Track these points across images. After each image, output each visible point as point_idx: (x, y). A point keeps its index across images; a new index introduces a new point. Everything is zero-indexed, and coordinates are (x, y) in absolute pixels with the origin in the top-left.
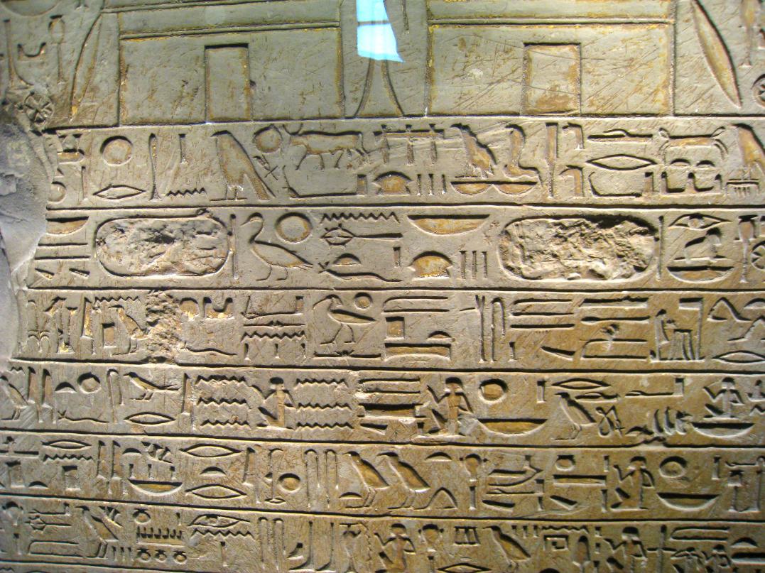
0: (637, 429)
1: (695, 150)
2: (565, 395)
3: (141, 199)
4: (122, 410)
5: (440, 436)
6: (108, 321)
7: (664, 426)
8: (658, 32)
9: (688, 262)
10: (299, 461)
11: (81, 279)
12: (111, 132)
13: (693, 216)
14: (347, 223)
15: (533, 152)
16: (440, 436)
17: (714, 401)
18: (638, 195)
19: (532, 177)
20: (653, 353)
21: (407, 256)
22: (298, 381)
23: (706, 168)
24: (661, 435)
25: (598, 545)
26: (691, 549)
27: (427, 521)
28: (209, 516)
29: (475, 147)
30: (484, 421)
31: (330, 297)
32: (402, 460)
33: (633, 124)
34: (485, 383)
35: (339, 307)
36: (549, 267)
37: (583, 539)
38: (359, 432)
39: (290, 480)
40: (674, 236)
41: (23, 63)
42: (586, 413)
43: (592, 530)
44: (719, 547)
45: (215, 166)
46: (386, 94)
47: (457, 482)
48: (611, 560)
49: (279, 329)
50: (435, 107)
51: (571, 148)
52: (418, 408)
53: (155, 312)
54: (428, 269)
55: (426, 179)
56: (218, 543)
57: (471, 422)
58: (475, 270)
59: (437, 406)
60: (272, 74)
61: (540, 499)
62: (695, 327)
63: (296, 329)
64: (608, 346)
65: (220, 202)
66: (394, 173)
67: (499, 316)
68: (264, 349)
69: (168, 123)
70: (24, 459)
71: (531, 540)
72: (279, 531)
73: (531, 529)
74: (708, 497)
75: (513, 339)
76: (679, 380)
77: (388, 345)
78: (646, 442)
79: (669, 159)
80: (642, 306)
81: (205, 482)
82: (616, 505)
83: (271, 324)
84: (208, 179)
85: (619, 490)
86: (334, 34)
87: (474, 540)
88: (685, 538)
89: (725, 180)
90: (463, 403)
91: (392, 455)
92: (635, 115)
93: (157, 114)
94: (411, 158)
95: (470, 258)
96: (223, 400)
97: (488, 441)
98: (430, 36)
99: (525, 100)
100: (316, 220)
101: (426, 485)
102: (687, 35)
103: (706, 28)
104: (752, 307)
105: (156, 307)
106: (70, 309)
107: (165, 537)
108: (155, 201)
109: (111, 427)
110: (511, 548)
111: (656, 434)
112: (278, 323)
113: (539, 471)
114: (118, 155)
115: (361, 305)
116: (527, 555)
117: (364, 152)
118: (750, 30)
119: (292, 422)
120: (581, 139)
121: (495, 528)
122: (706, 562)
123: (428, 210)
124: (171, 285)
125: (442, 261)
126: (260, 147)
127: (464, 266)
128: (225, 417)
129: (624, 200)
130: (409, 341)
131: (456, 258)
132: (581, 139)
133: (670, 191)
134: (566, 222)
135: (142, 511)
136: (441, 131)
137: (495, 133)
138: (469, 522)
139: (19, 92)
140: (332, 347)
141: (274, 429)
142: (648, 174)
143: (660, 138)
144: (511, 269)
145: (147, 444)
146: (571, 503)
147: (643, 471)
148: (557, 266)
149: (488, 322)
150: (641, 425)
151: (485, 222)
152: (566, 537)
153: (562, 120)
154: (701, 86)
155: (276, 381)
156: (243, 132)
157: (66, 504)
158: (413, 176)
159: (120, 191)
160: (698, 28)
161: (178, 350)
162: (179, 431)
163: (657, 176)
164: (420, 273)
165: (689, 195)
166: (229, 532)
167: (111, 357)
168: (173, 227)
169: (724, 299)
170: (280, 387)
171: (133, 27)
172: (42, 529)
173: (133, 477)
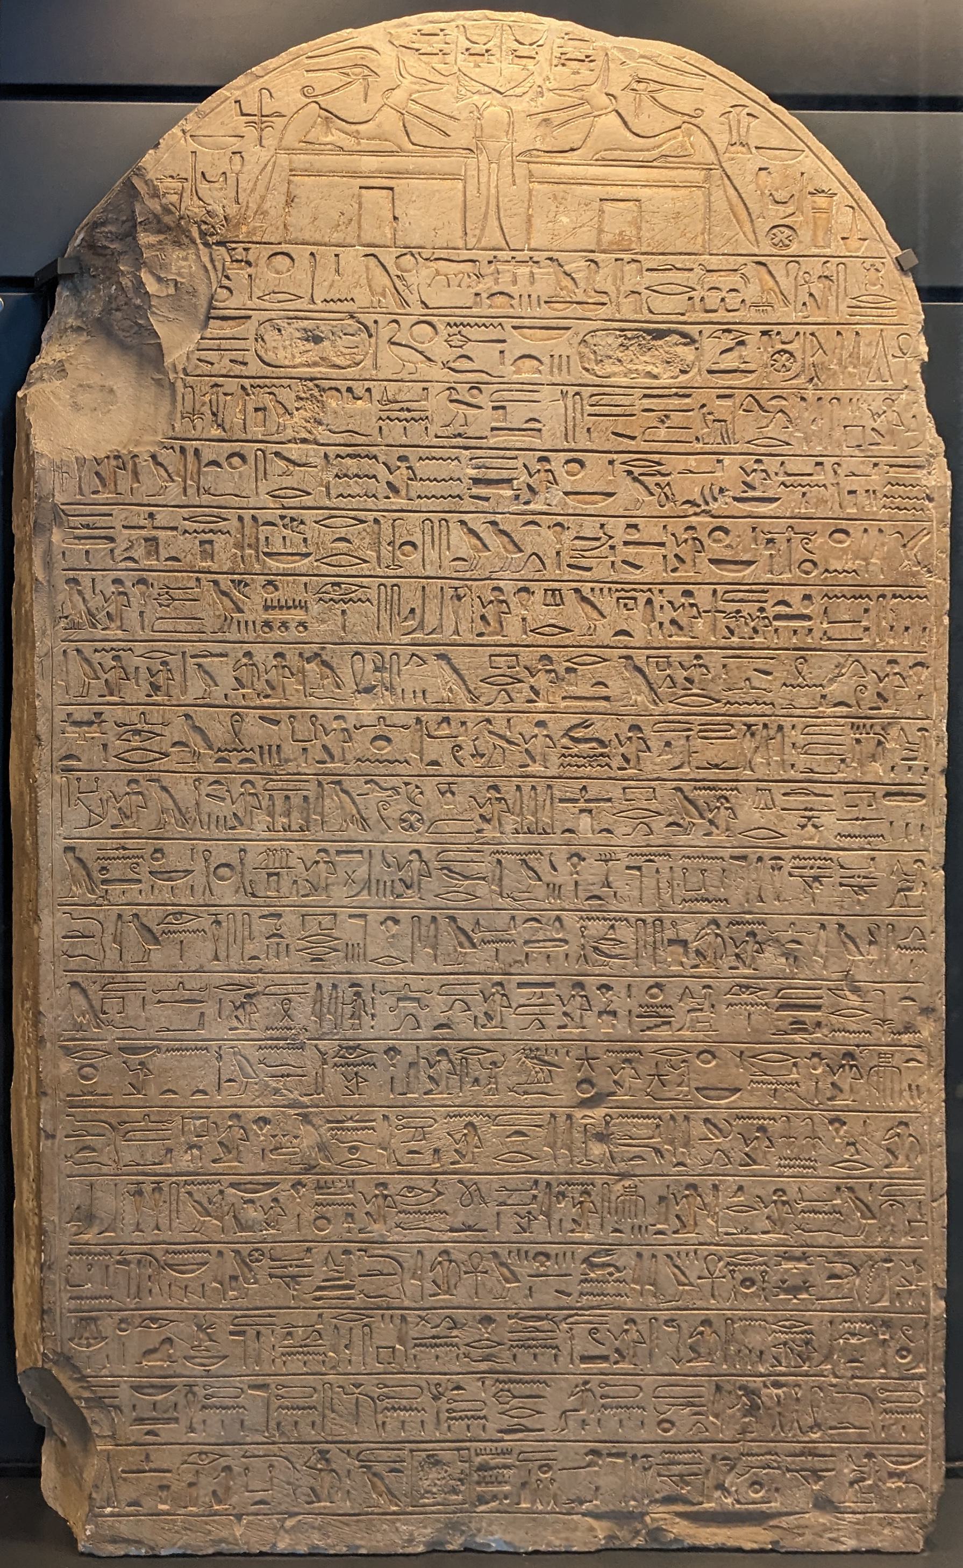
0: (687, 502)
1: (726, 281)
2: (630, 473)
3: (298, 304)
4: (264, 487)
5: (532, 507)
6: (261, 406)
7: (710, 500)
8: (699, 193)
9: (722, 367)
10: (418, 529)
11: (238, 369)
12: (278, 248)
13: (724, 331)
14: (465, 331)
15: (603, 279)
16: (532, 507)
17: (748, 479)
18: (683, 314)
19: (605, 299)
20: (697, 439)
21: (509, 359)
22: (421, 458)
23: (734, 294)
24: (707, 508)
25: (662, 607)
26: (738, 612)
27: (521, 584)
28: (333, 584)
29: (562, 276)
30: (566, 494)
31: (449, 389)
32: (501, 527)
33: (679, 261)
34: (568, 462)
35: (455, 397)
36: (616, 369)
37: (649, 602)
38: (468, 504)
39: (408, 548)
40: (711, 347)
41: (203, 186)
42: (647, 488)
43: (656, 592)
44: (762, 610)
45: (364, 281)
46: (498, 233)
47: (546, 547)
48: (673, 622)
49: (407, 415)
50: (533, 245)
51: (633, 278)
52: (515, 482)
53: (302, 399)
54: (524, 369)
55: (525, 299)
56: (339, 612)
57: (556, 495)
58: (560, 370)
59: (531, 481)
60: (411, 212)
61: (613, 563)
62: (729, 418)
63: (423, 414)
64: (662, 433)
65: (365, 310)
66: (501, 293)
67: (578, 406)
68: (395, 432)
69: (325, 245)
70: (161, 534)
71: (607, 603)
72: (396, 597)
73: (606, 591)
74: (749, 563)
75: (590, 425)
76: (719, 461)
77: (493, 429)
78: (696, 514)
79: (706, 287)
80: (687, 400)
81: (334, 552)
82: (675, 570)
83: (402, 410)
84: (356, 291)
85: (676, 556)
86: (460, 185)
87: (558, 601)
88: (733, 601)
89: (748, 303)
90: (551, 478)
91: (493, 523)
92: (680, 254)
93: (317, 237)
94: (515, 282)
95: (556, 361)
96: (357, 476)
97: (571, 511)
98: (530, 191)
99: (599, 241)
100: (441, 327)
101: (521, 551)
102: (717, 194)
103: (731, 191)
104: (773, 402)
105: (303, 395)
106: (226, 394)
107: (289, 608)
108: (312, 307)
109: (252, 502)
110: (588, 608)
111: (703, 508)
112: (409, 410)
113: (611, 537)
114: (280, 268)
115: (473, 396)
116: (604, 617)
117: (479, 276)
118: (762, 194)
119: (413, 494)
120: (640, 271)
121: (577, 591)
122: (752, 624)
123: (527, 322)
124: (319, 376)
125: (535, 362)
126: (398, 267)
127: (552, 367)
128: (357, 490)
129: (673, 318)
130: (509, 426)
131: (546, 360)
132: (640, 271)
133: (707, 311)
134: (629, 334)
135: (270, 583)
136: (537, 262)
137: (576, 265)
138: (556, 585)
139: (197, 210)
140: (450, 430)
141: (398, 502)
142: (690, 299)
143: (698, 271)
144: (587, 370)
145: (282, 517)
146: (638, 567)
147: (695, 539)
148: (622, 368)
149: (570, 411)
150: (691, 499)
151: (570, 332)
152: (635, 599)
153: (627, 257)
154: (729, 234)
155: (402, 458)
156: (388, 257)
157: (198, 580)
158: (517, 296)
159: (281, 297)
160: (725, 192)
161: (321, 433)
162: (315, 505)
163: (697, 300)
164: (518, 372)
165: (721, 315)
166: (351, 600)
167: (260, 437)
168: (325, 328)
169: (751, 395)
170: (403, 465)
171: (302, 166)
172: (168, 606)
173: (266, 550)
